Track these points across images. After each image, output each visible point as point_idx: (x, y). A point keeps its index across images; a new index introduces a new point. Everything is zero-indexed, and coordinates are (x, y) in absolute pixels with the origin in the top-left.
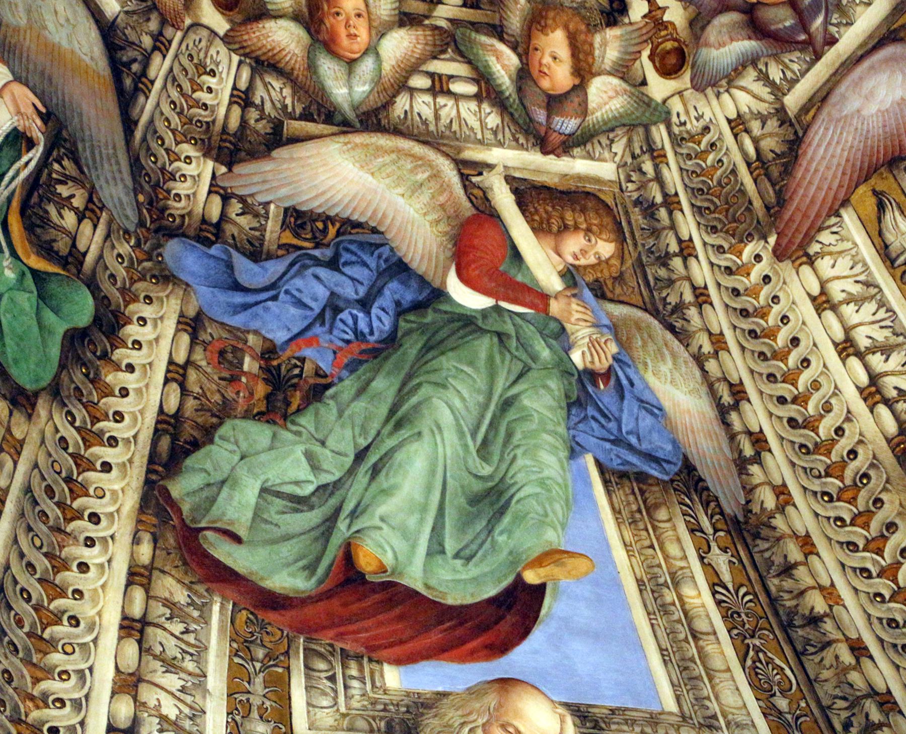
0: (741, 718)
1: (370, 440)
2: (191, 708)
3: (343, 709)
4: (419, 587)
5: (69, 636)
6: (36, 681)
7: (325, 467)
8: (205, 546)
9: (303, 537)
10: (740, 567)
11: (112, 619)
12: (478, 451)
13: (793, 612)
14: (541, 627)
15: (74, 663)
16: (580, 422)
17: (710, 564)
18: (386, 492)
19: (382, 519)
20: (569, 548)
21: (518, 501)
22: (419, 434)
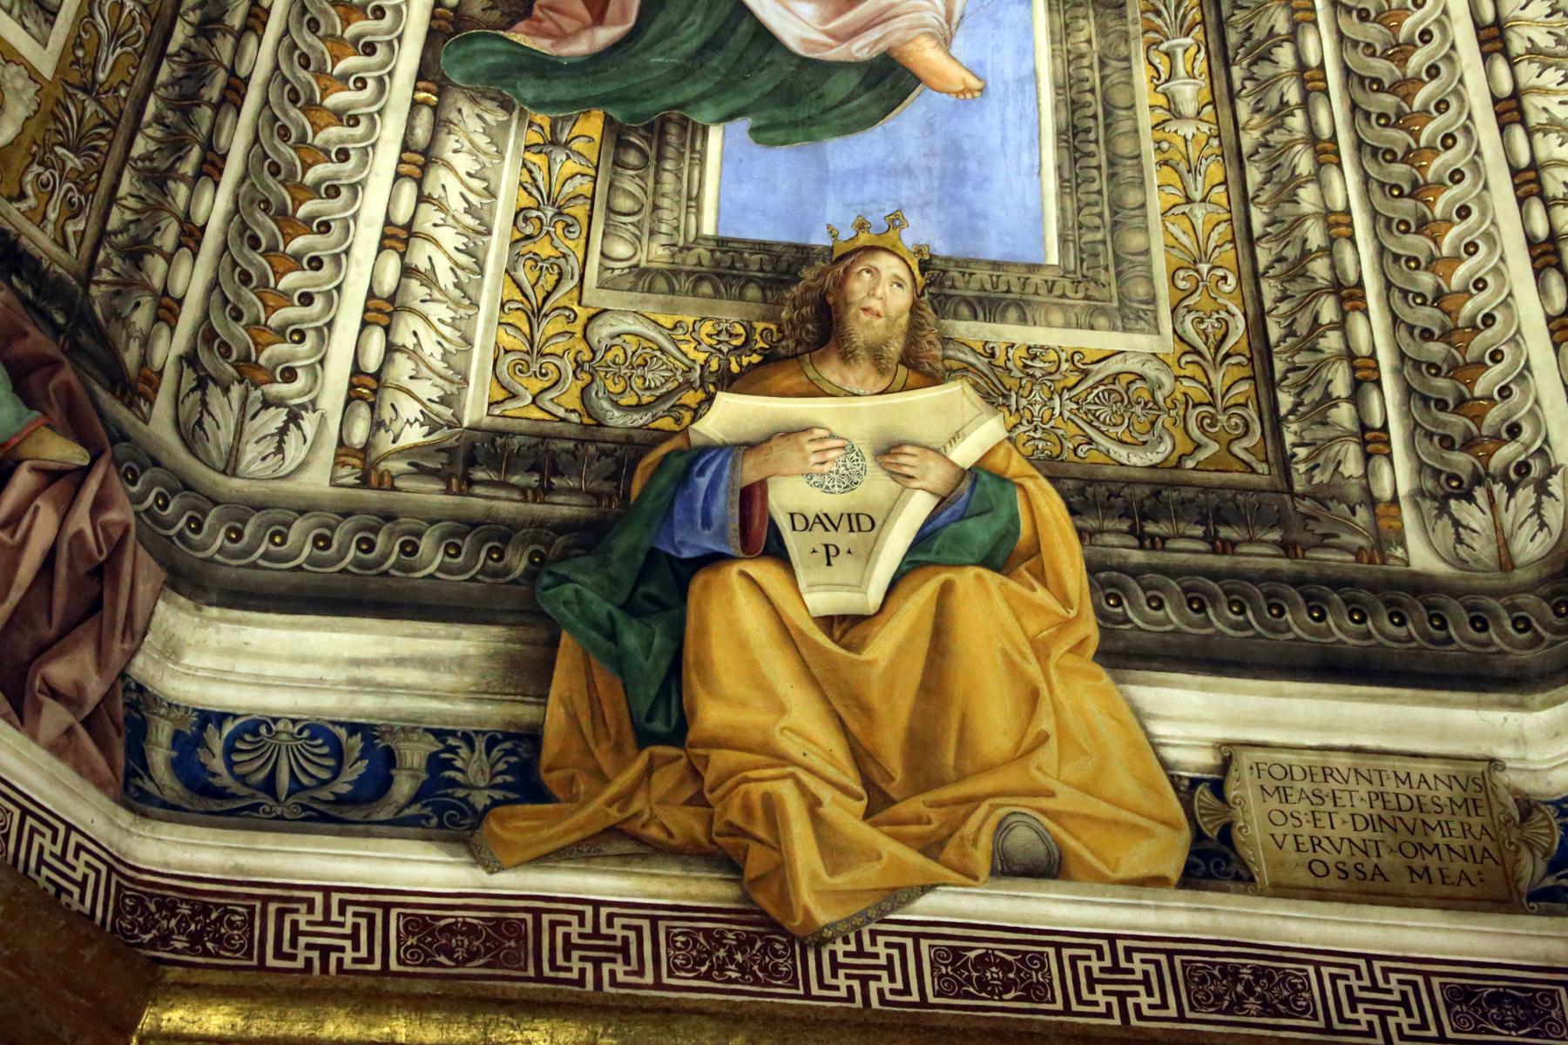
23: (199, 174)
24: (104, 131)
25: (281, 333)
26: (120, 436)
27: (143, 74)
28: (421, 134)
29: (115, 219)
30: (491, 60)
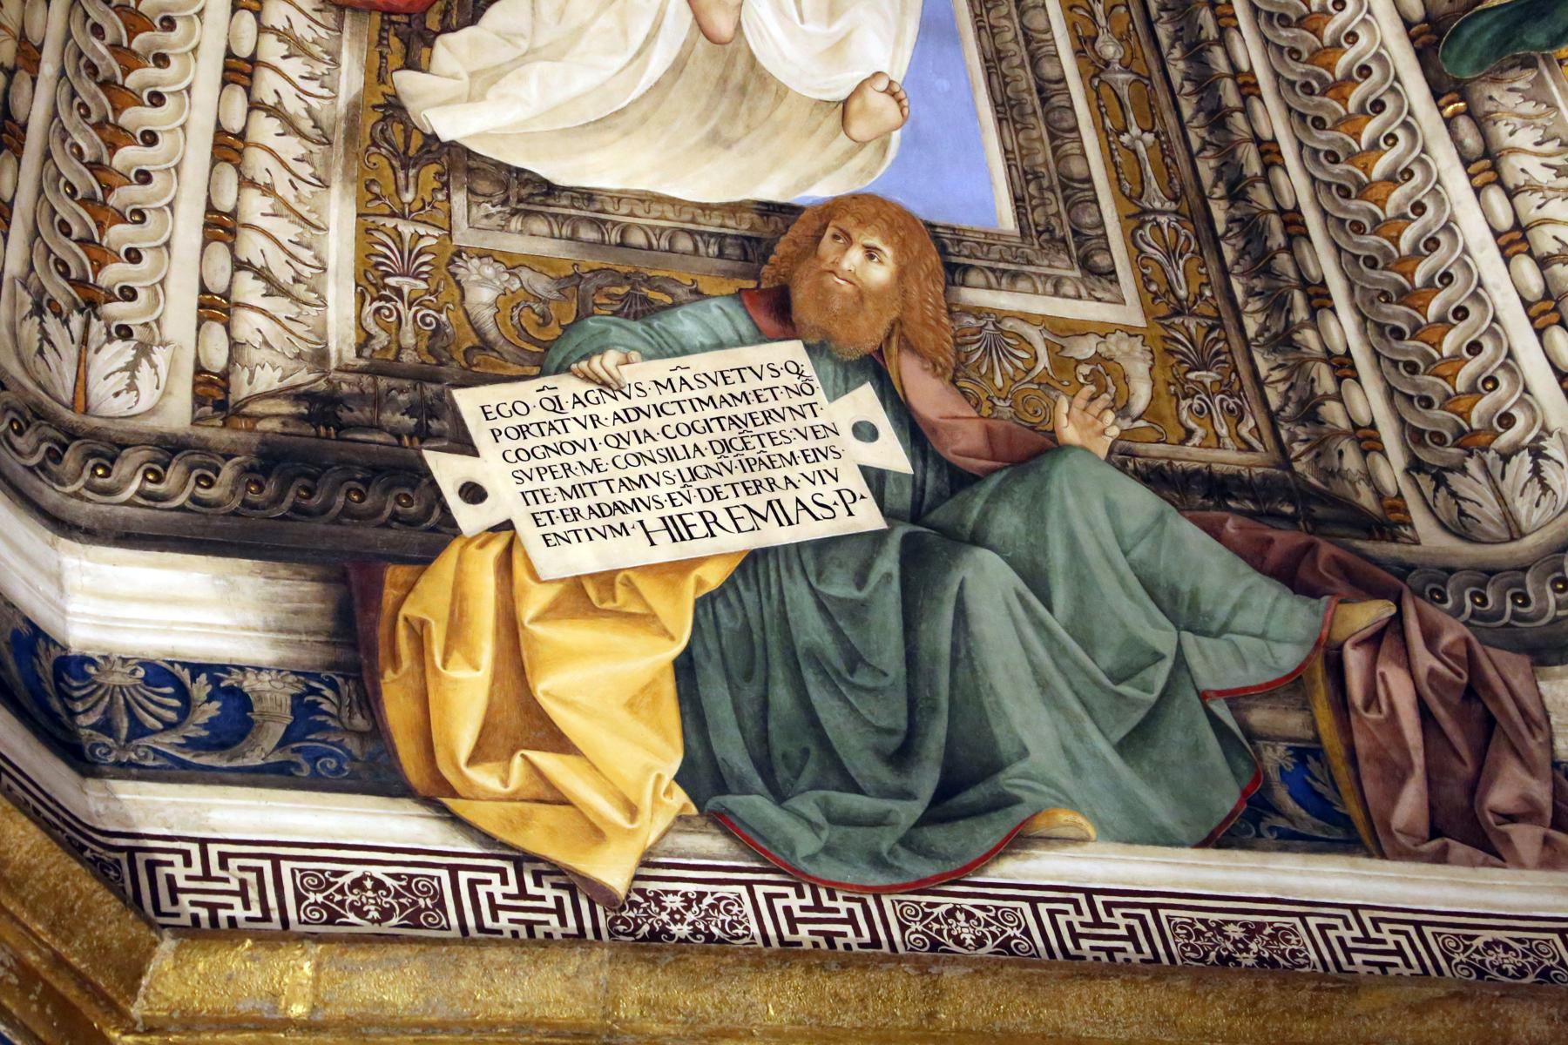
23: (1313, 313)
24: (1214, 334)
25: (1473, 391)
26: (1405, 569)
27: (1213, 267)
28: (1472, 141)
29: (1274, 401)
30: (1488, 36)
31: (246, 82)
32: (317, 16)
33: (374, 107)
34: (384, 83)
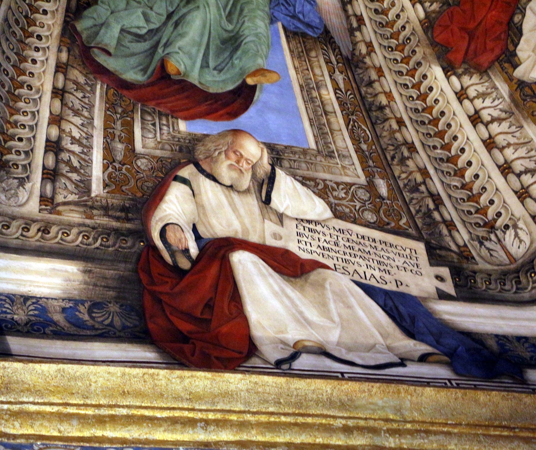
0: (345, 153)
1: (174, 8)
2: (86, 134)
3: (159, 140)
4: (196, 83)
5: (27, 94)
6: (12, 115)
7: (152, 20)
8: (93, 56)
9: (141, 55)
10: (349, 81)
11: (48, 88)
12: (226, 18)
13: (371, 104)
14: (254, 106)
15: (30, 108)
16: (276, 6)
17: (334, 79)
18: (182, 36)
19: (179, 48)
20: (269, 68)
21: (245, 44)
22: (198, 7)
31: (479, 120)
32: (482, 81)
33: (516, 90)
34: (513, 80)
